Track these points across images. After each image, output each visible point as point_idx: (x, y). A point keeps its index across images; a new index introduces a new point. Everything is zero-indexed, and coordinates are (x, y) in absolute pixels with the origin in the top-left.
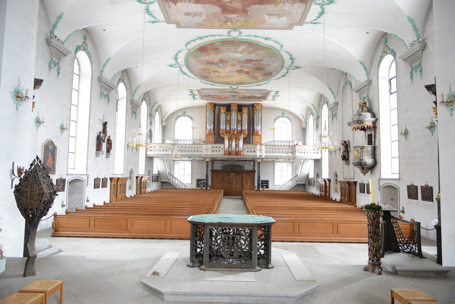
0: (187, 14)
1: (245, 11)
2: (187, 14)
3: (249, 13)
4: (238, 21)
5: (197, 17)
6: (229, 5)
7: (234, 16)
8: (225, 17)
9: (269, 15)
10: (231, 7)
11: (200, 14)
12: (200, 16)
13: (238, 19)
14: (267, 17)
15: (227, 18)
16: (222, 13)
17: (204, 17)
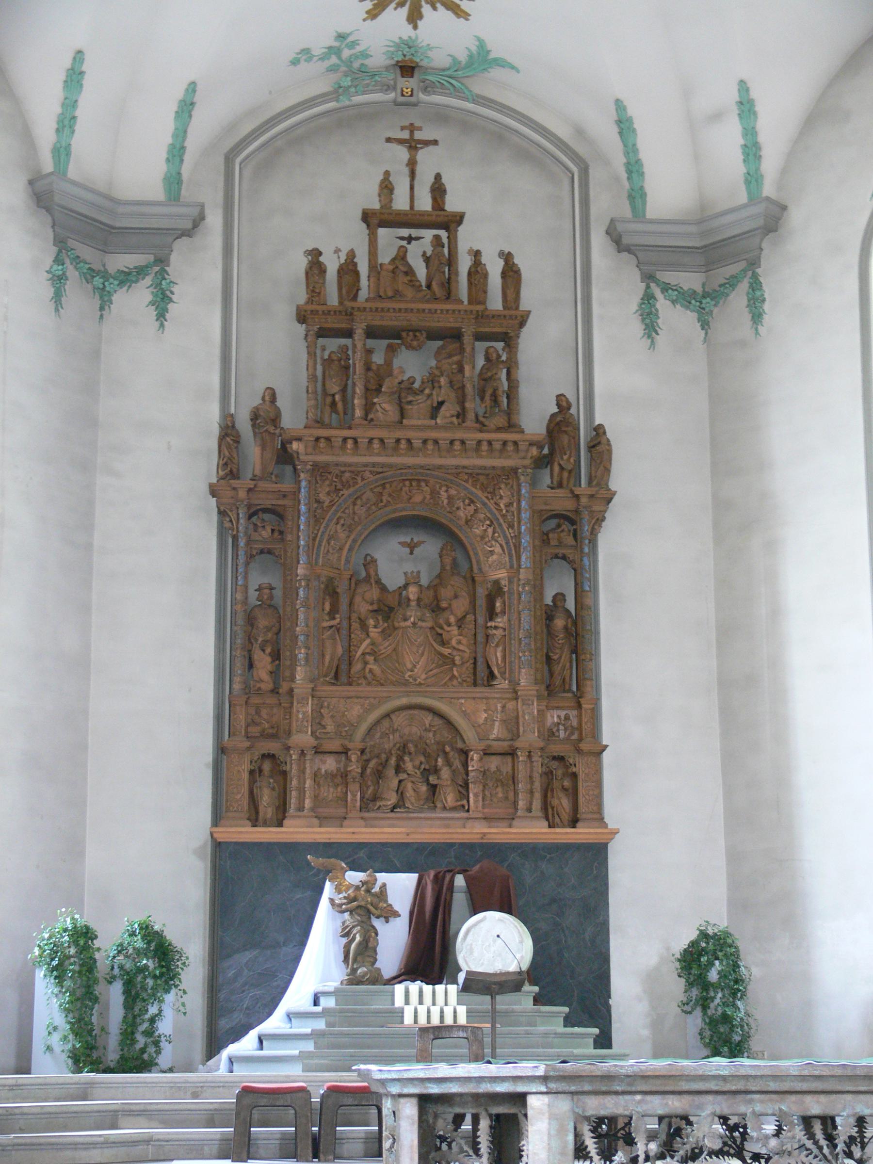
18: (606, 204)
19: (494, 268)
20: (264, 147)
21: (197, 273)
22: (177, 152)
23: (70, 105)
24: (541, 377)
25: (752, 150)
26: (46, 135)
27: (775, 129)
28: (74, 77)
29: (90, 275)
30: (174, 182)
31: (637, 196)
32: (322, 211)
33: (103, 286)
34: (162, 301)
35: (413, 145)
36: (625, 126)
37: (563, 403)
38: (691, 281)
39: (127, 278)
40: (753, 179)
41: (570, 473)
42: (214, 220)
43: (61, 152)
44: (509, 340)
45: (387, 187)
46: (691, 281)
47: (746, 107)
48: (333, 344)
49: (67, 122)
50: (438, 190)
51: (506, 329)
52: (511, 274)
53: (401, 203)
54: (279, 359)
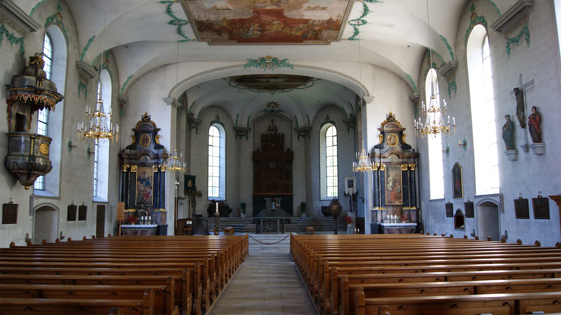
0: (324, 9)
1: (258, 12)
2: (324, 9)
3: (252, 11)
4: (264, 3)
5: (312, 6)
6: (274, 18)
7: (269, 8)
8: (280, 7)
9: (227, 9)
10: (272, 16)
11: (309, 8)
12: (309, 7)
13: (263, 5)
14: (229, 6)
15: (277, 5)
16: (283, 10)
17: (305, 6)
18: (294, 126)
19: (281, 134)
20: (257, 120)
21: (250, 135)
22: (248, 122)
23: (237, 119)
24: (287, 145)
25: (309, 121)
26: (235, 122)
27: (311, 118)
28: (237, 116)
29: (239, 135)
30: (248, 125)
31: (297, 125)
32: (263, 128)
33: (241, 136)
34: (247, 138)
35: (273, 121)
36: (296, 117)
37: (288, 149)
38: (303, 134)
39: (243, 135)
40: (309, 123)
41: (289, 156)
42: (252, 129)
43: (236, 124)
44: (283, 142)
45: (270, 126)
46: (303, 134)
47: (308, 116)
48: (265, 143)
49: (237, 121)
50: (275, 126)
51: (283, 140)
52: (283, 135)
53: (271, 128)
54: (258, 144)
